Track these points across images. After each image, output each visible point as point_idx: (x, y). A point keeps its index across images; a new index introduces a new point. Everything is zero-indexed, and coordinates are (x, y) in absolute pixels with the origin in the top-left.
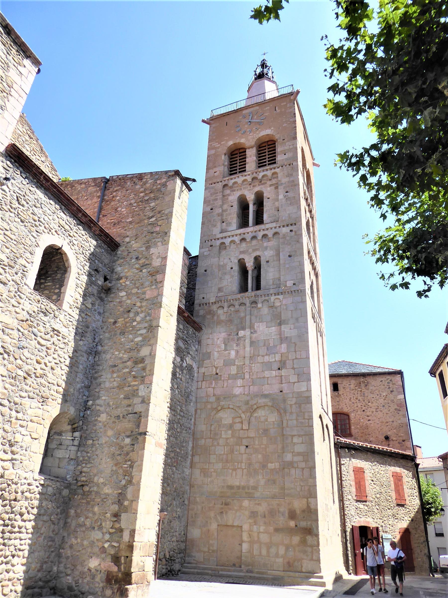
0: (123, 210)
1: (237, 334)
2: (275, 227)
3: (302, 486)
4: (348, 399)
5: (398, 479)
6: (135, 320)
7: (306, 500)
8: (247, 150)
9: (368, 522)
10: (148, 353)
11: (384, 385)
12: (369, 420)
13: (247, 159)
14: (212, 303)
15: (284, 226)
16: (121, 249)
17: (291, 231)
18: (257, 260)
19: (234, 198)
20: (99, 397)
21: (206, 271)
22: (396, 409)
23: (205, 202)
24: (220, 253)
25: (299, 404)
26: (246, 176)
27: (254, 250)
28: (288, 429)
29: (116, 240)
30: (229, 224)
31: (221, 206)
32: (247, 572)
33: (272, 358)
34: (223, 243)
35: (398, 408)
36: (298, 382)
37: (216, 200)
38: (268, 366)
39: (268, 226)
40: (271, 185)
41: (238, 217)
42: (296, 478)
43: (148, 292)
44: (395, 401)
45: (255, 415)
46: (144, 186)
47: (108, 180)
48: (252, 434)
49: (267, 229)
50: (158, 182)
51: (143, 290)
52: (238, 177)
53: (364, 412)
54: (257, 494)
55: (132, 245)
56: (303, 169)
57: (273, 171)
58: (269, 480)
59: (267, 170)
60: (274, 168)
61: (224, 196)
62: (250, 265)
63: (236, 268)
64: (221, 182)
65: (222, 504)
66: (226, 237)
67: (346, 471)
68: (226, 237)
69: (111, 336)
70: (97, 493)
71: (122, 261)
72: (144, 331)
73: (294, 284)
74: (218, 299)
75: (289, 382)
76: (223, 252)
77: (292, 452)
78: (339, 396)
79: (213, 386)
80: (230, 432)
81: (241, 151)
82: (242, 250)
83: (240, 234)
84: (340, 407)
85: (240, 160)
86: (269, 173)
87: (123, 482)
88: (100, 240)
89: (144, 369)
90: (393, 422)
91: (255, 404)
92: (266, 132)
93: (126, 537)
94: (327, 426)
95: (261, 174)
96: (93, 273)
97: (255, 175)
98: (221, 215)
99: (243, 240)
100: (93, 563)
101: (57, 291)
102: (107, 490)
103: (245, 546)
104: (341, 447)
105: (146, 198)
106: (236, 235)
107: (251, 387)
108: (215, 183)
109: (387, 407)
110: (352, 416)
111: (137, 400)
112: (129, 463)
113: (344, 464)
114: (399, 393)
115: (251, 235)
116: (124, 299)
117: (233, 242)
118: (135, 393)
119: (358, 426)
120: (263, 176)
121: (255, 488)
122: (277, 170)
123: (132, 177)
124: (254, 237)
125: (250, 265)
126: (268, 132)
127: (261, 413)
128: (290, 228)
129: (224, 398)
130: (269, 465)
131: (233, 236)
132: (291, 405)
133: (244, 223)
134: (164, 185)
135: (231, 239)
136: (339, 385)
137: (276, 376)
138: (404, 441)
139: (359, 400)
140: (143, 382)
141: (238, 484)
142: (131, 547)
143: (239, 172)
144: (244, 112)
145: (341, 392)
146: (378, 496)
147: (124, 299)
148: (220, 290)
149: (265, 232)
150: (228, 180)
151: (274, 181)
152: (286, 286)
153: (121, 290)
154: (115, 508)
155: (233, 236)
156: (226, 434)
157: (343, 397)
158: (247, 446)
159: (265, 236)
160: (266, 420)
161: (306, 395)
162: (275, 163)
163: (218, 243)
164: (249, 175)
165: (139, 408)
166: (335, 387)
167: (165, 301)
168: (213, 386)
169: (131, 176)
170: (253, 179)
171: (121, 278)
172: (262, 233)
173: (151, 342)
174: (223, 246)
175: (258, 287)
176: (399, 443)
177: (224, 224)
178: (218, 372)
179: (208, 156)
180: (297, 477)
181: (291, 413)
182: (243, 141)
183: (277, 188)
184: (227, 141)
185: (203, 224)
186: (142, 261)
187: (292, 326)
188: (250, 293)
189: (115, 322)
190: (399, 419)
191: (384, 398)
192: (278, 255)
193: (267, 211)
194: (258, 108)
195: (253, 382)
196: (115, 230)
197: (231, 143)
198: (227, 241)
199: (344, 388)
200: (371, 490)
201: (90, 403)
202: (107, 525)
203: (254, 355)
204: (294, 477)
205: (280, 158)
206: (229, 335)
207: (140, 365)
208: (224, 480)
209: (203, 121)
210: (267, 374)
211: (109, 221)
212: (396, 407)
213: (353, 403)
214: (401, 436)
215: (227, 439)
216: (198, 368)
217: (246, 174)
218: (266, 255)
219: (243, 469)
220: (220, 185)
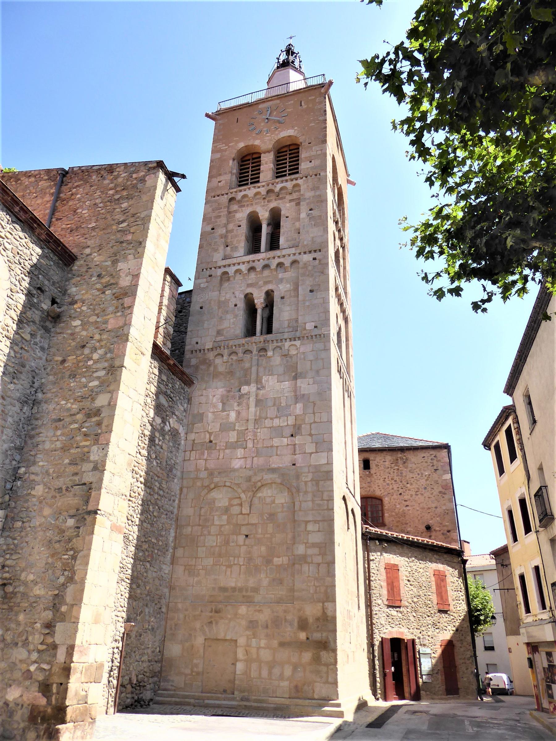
0: (83, 212)
1: (240, 390)
2: (294, 254)
3: (316, 587)
4: (382, 480)
5: (440, 578)
6: (91, 359)
7: (321, 604)
8: (262, 155)
9: (402, 633)
10: (106, 403)
11: (426, 462)
12: (407, 506)
13: (261, 167)
14: (208, 349)
15: (305, 253)
16: (77, 263)
17: (314, 259)
18: (269, 295)
19: (242, 215)
20: (34, 463)
21: (201, 308)
22: (440, 492)
23: (204, 220)
24: (221, 284)
25: (316, 482)
26: (259, 187)
27: (266, 283)
28: (301, 513)
29: (72, 251)
30: (235, 249)
31: (226, 226)
32: (242, 700)
33: (284, 421)
34: (226, 273)
35: (443, 491)
36: (317, 452)
38: (278, 431)
39: (284, 252)
40: (291, 201)
41: (247, 240)
42: (309, 576)
43: (112, 321)
44: (440, 481)
45: (259, 495)
46: (115, 182)
47: (67, 172)
48: (254, 520)
49: (284, 256)
50: (134, 176)
51: (105, 317)
52: (249, 189)
53: (401, 496)
54: (258, 598)
55: (93, 259)
56: (333, 184)
57: (295, 182)
58: (274, 580)
59: (287, 181)
60: (296, 179)
61: (229, 213)
62: (259, 301)
63: (242, 305)
64: (227, 194)
65: (211, 612)
66: (229, 265)
67: (377, 568)
68: (229, 265)
69: (57, 379)
70: (25, 595)
71: (79, 279)
72: (102, 373)
73: (315, 327)
74: (216, 345)
75: (305, 453)
76: (226, 285)
77: (306, 543)
78: (370, 475)
79: (205, 457)
80: (225, 517)
81: (254, 156)
82: (250, 282)
83: (248, 262)
84: (372, 490)
85: (252, 167)
86: (289, 185)
87: (62, 580)
88: (48, 248)
89: (99, 424)
90: (436, 508)
91: (259, 481)
92: (287, 133)
93: (61, 655)
94: (352, 510)
96: (35, 292)
97: (271, 187)
99: (252, 269)
100: (13, 694)
102: (38, 591)
103: (240, 666)
104: (371, 539)
105: (117, 197)
106: (244, 263)
107: (255, 459)
108: (218, 196)
109: (430, 489)
110: (386, 500)
111: (87, 467)
112: (71, 553)
113: (373, 560)
114: (445, 472)
115: (262, 263)
116: (77, 330)
117: (238, 271)
118: (84, 457)
119: (394, 514)
120: (281, 189)
121: (256, 590)
122: (300, 181)
123: (99, 169)
124: (266, 266)
125: (259, 301)
126: (290, 132)
127: (266, 493)
129: (219, 473)
130: (275, 559)
131: (239, 264)
132: (306, 482)
133: (254, 248)
134: (143, 180)
135: (237, 267)
136: (371, 462)
137: (288, 445)
138: (449, 531)
139: (396, 481)
141: (233, 585)
142: (67, 671)
143: (251, 183)
144: (261, 106)
145: (373, 470)
146: (415, 600)
147: (77, 330)
148: (219, 333)
149: (281, 260)
150: (236, 192)
151: (295, 196)
152: (305, 329)
153: (75, 318)
154: (48, 615)
155: (239, 264)
156: (220, 520)
157: (375, 477)
158: (247, 536)
159: (280, 265)
160: (273, 502)
161: (326, 469)
162: (298, 173)
163: (219, 272)
164: (263, 186)
165: (88, 478)
166: (366, 465)
167: (133, 332)
168: (205, 457)
169: (98, 167)
170: (269, 192)
171: (76, 302)
172: (277, 261)
173: (111, 388)
175: (269, 331)
176: (443, 534)
177: (229, 248)
178: (212, 439)
179: (212, 161)
180: (310, 575)
181: (306, 492)
182: (257, 142)
183: (298, 204)
184: (237, 142)
185: (201, 247)
186: (105, 280)
187: (311, 381)
188: (259, 338)
189: (63, 361)
190: (445, 505)
191: (426, 478)
192: (296, 289)
193: (284, 234)
194: (278, 101)
195: (257, 453)
196: (71, 238)
197: (241, 145)
198: (231, 270)
199: (377, 466)
200: (406, 592)
201: (22, 470)
202: (36, 639)
203: (260, 418)
204: (307, 575)
205: (304, 166)
206: (229, 391)
207: (94, 419)
208: (215, 580)
209: (207, 115)
210: (276, 442)
211: (64, 226)
212: (440, 489)
213: (388, 484)
214: (446, 526)
215: (221, 526)
216: (186, 434)
217: (259, 185)
218: (281, 289)
219: (240, 566)
220: (225, 199)
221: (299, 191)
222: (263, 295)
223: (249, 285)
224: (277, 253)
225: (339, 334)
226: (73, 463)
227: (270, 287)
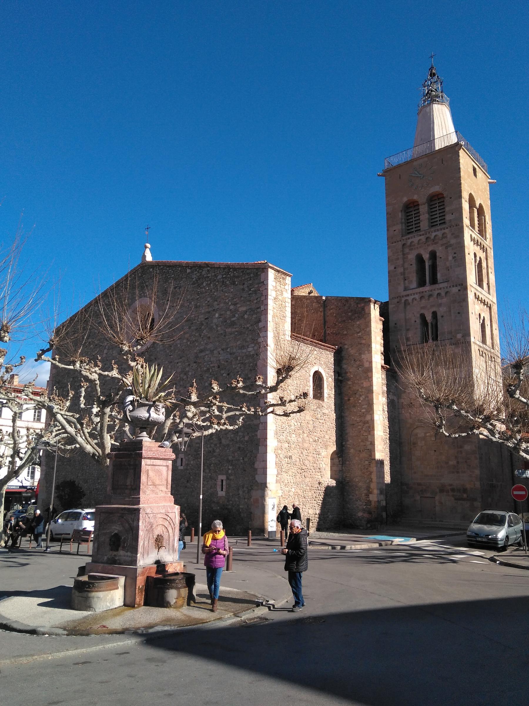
2: (447, 287)
6: (360, 400)
8: (420, 207)
10: (370, 419)
15: (453, 286)
18: (435, 314)
19: (412, 256)
20: (348, 441)
21: (396, 324)
26: (420, 235)
27: (432, 306)
31: (403, 265)
32: (440, 521)
37: (398, 259)
39: (442, 285)
40: (442, 245)
41: (417, 273)
43: (364, 383)
49: (441, 289)
57: (443, 231)
59: (438, 230)
61: (404, 254)
63: (419, 321)
64: (400, 241)
68: (408, 295)
72: (365, 406)
76: (408, 307)
80: (423, 442)
81: (415, 204)
82: (422, 306)
85: (415, 214)
86: (439, 234)
87: (368, 481)
89: (369, 427)
92: (436, 189)
95: (434, 234)
97: (428, 235)
98: (403, 274)
99: (421, 298)
100: (360, 514)
102: (360, 484)
103: (438, 509)
106: (417, 293)
108: (395, 242)
118: (367, 439)
120: (435, 236)
122: (446, 231)
125: (429, 318)
128: (459, 288)
133: (422, 283)
134: (363, 309)
135: (412, 297)
140: (369, 434)
144: (415, 163)
149: (439, 291)
150: (406, 239)
151: (444, 241)
159: (439, 294)
163: (403, 300)
165: (369, 447)
167: (375, 388)
170: (427, 238)
173: (371, 413)
174: (406, 303)
177: (406, 282)
179: (387, 214)
182: (415, 197)
185: (390, 281)
186: (358, 363)
192: (450, 311)
194: (426, 159)
197: (405, 199)
198: (410, 298)
201: (344, 443)
205: (448, 217)
207: (367, 425)
215: (422, 447)
216: (398, 399)
217: (421, 233)
218: (441, 311)
220: (400, 244)
221: (446, 237)
222: (431, 315)
223: (422, 308)
224: (436, 286)
225: (483, 326)
226: (362, 441)
227: (434, 309)
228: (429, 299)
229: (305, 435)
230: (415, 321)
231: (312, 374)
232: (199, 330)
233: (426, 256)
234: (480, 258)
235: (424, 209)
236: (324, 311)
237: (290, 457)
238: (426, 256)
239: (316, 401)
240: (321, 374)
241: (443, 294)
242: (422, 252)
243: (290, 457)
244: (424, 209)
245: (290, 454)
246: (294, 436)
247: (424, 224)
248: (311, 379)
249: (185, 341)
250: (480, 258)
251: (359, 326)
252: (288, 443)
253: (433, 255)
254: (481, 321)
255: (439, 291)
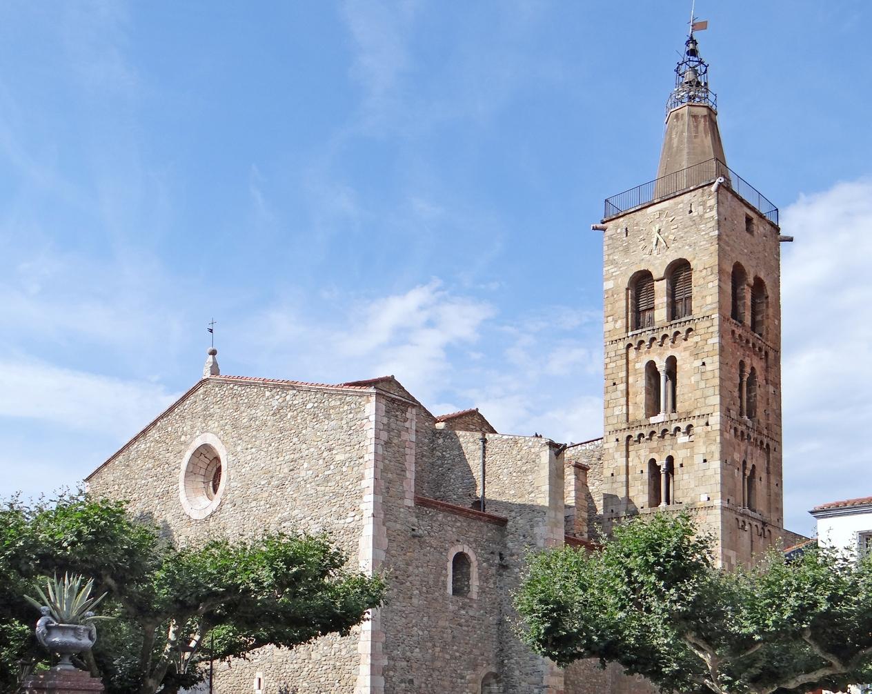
13: (655, 301)
16: (510, 523)
18: (670, 460)
19: (641, 366)
40: (685, 349)
50: (533, 450)
55: (518, 521)
101: (466, 583)
105: (524, 469)
149: (678, 424)
186: (529, 539)
211: (493, 490)
228: (650, 439)
229: (438, 649)
230: (642, 472)
231: (451, 559)
232: (281, 486)
233: (661, 366)
234: (753, 369)
235: (661, 288)
236: (484, 457)
237: (411, 681)
238: (661, 366)
239: (456, 598)
240: (469, 558)
241: (683, 429)
242: (656, 359)
243: (411, 681)
244: (661, 288)
245: (410, 677)
246: (417, 650)
247: (661, 314)
248: (450, 565)
249: (262, 503)
250: (753, 369)
251: (531, 484)
252: (408, 661)
253: (672, 361)
254: (748, 473)
255: (678, 424)
